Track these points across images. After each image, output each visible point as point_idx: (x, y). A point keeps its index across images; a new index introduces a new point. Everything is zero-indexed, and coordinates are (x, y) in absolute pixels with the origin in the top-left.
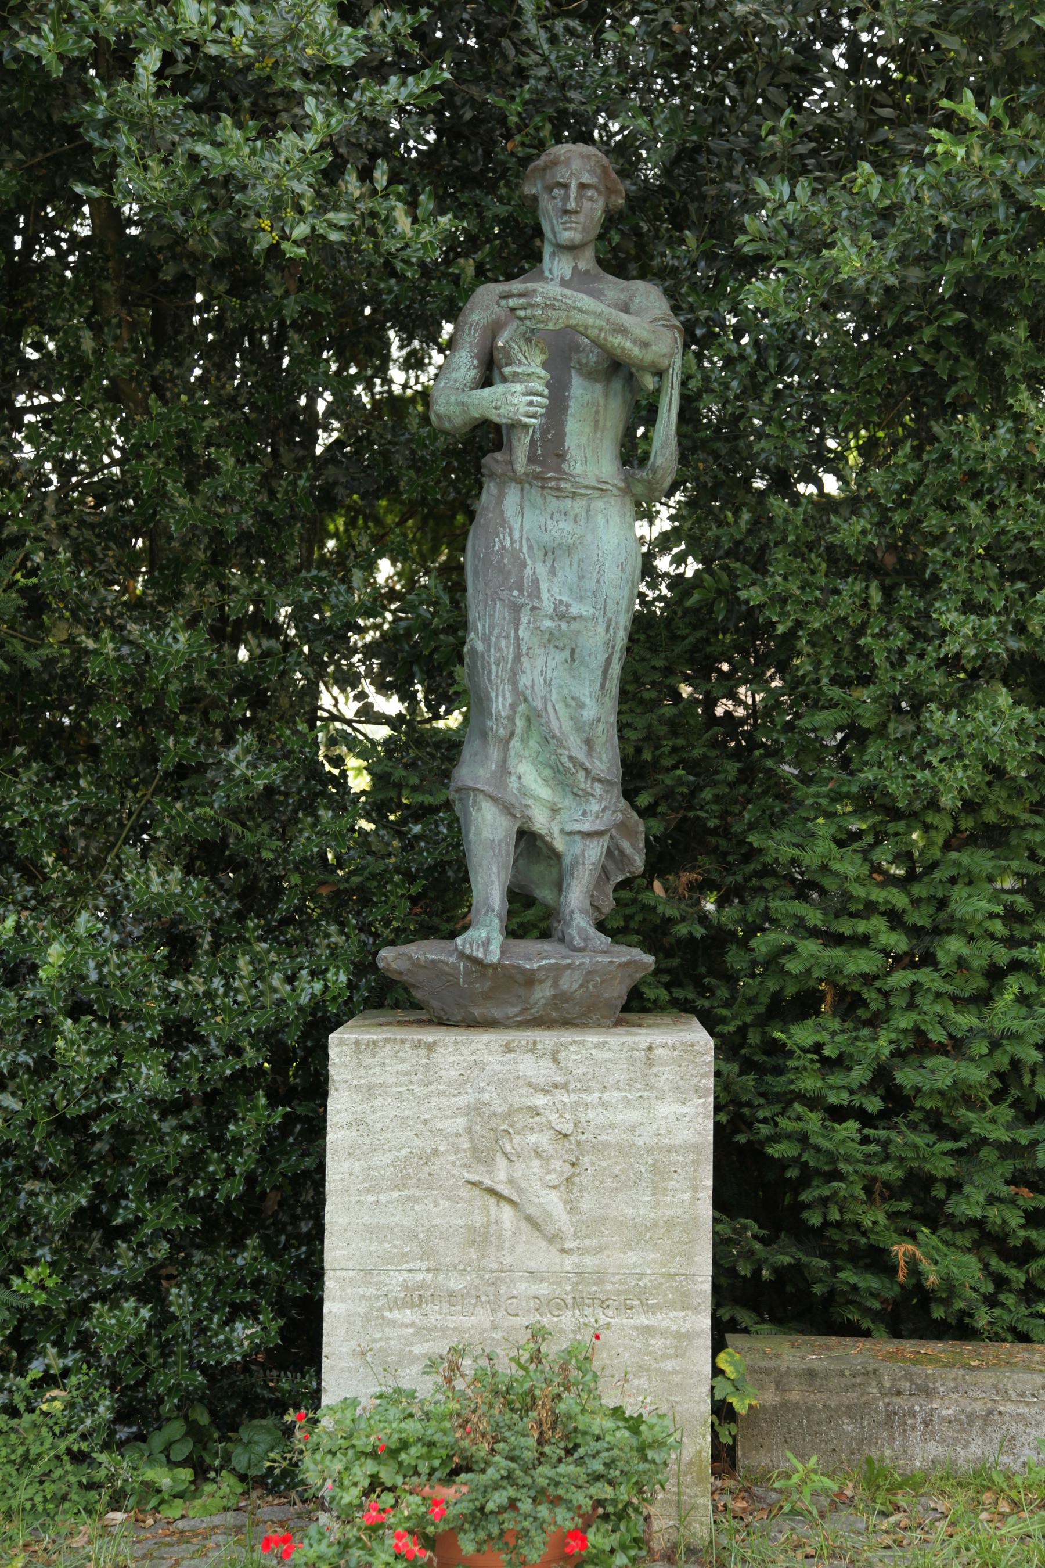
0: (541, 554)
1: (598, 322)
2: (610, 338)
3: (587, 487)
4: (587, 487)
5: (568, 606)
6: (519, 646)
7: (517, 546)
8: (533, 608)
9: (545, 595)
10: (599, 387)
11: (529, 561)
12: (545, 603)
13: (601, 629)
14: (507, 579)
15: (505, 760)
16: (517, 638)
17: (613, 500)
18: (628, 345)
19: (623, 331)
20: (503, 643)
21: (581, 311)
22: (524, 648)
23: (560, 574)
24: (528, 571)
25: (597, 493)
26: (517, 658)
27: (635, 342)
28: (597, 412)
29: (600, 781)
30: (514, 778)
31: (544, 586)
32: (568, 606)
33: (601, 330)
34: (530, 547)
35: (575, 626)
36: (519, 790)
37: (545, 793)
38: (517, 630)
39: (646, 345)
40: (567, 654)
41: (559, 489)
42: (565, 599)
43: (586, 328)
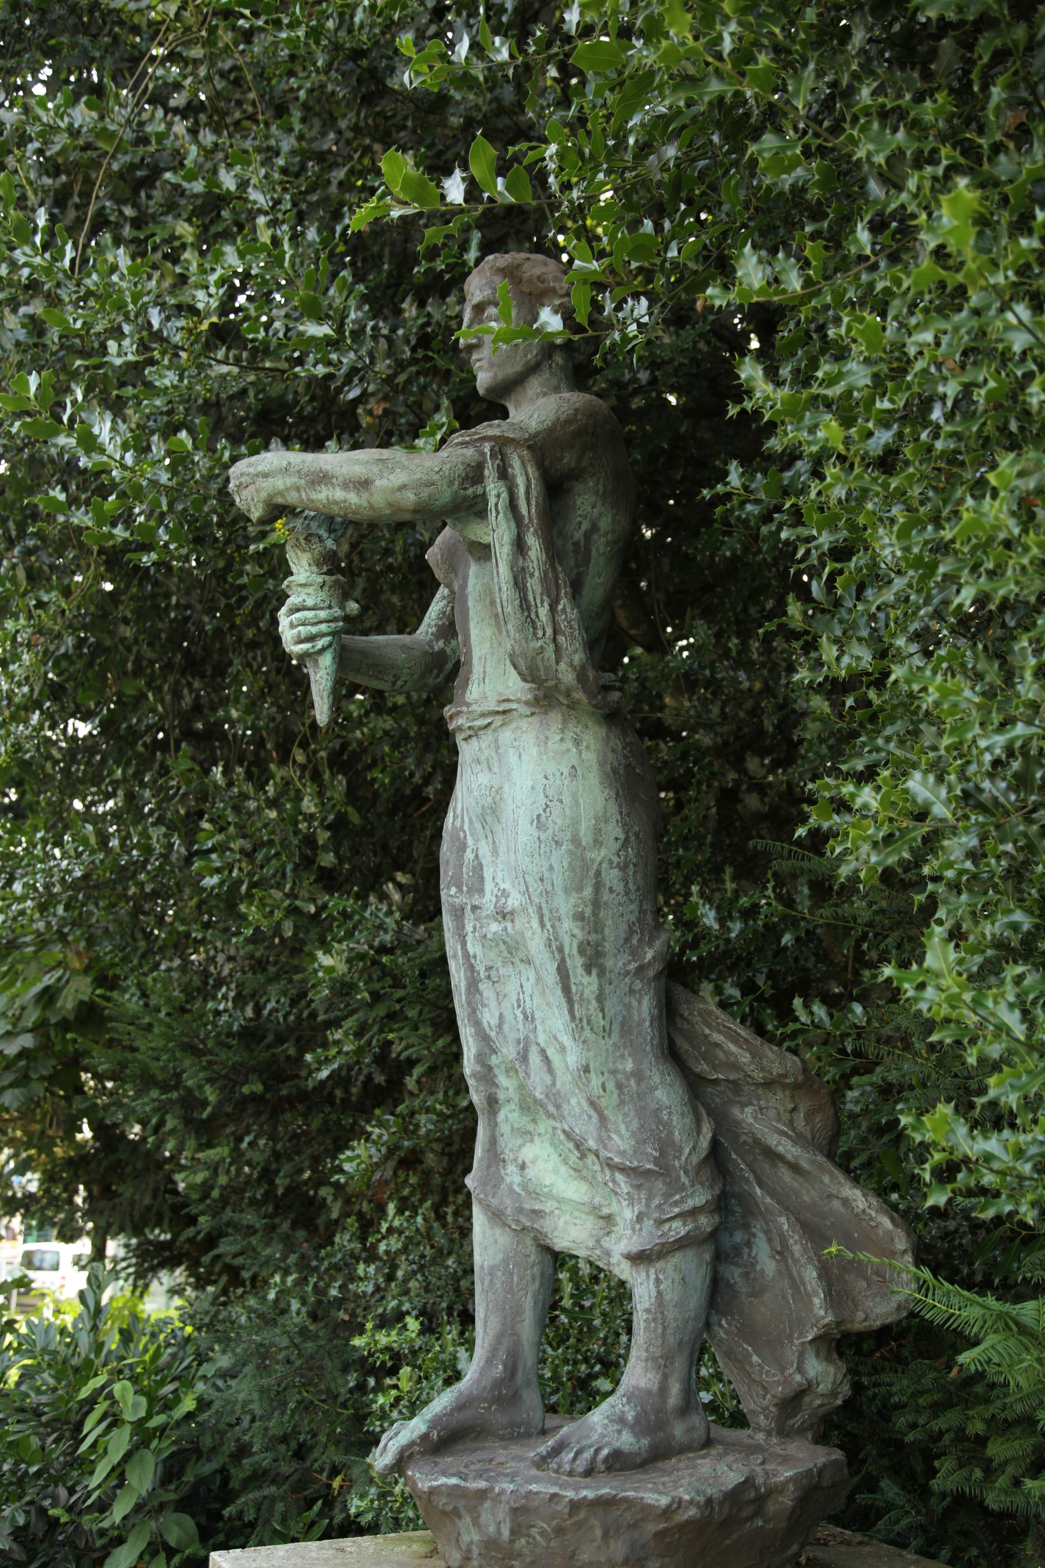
1: (290, 481)
2: (314, 496)
3: (483, 715)
4: (483, 715)
6: (471, 968)
7: (458, 824)
8: (475, 908)
9: (489, 886)
11: (470, 841)
16: (466, 955)
17: (524, 724)
18: (339, 494)
19: (323, 478)
21: (266, 475)
22: (481, 968)
24: (469, 855)
25: (498, 720)
26: (473, 985)
27: (346, 486)
30: (511, 1168)
31: (488, 873)
33: (298, 489)
34: (471, 821)
36: (524, 1186)
37: (574, 1190)
38: (464, 944)
39: (364, 484)
43: (280, 493)
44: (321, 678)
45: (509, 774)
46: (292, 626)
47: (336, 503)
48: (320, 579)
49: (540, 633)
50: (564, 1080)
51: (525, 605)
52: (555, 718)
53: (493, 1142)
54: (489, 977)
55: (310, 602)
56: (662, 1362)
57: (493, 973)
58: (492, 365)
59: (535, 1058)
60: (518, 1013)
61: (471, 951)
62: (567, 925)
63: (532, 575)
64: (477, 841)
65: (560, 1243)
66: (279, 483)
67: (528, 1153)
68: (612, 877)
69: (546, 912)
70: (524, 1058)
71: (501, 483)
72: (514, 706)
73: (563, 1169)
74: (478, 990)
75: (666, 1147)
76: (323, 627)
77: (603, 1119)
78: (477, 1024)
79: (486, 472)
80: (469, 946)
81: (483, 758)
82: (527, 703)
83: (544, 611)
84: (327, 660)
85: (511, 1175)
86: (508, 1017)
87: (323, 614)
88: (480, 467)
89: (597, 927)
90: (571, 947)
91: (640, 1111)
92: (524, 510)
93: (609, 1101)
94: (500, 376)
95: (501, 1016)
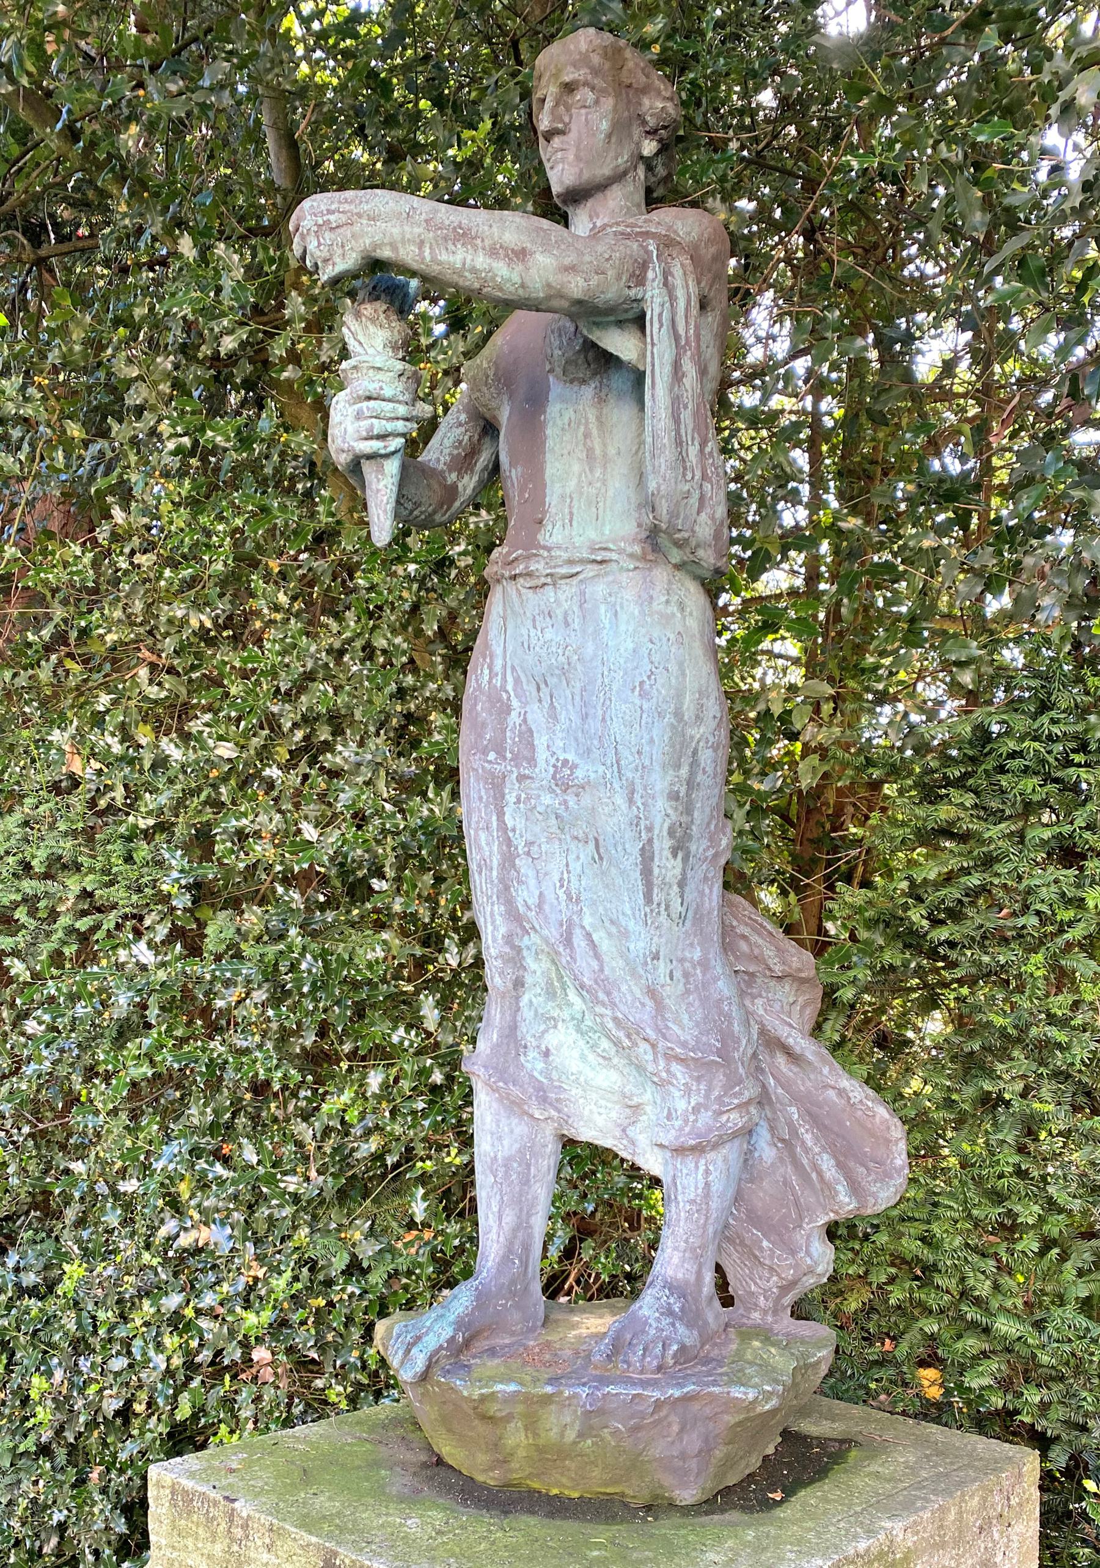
0: (533, 688)
2: (443, 257)
3: (571, 562)
4: (571, 562)
5: (574, 767)
9: (542, 755)
10: (588, 391)
11: (515, 703)
12: (541, 764)
13: (620, 800)
14: (480, 736)
15: (514, 1027)
17: (624, 578)
18: (481, 261)
20: (483, 836)
23: (562, 717)
24: (514, 718)
25: (591, 570)
26: (509, 860)
27: (492, 252)
28: (587, 435)
29: (682, 1061)
31: (541, 741)
32: (574, 767)
34: (517, 681)
35: (587, 800)
38: (501, 815)
39: (521, 255)
40: (592, 845)
41: (529, 575)
42: (571, 757)
44: (382, 488)
45: (597, 633)
46: (359, 416)
47: (474, 270)
48: (400, 366)
49: (689, 476)
50: (615, 966)
51: (679, 442)
52: (661, 575)
53: (511, 1031)
54: (528, 854)
55: (388, 392)
56: (695, 1254)
57: (534, 849)
58: (578, 158)
59: (579, 941)
60: (561, 893)
61: (510, 824)
62: (661, 804)
63: (686, 407)
64: (525, 704)
65: (585, 1134)
66: (396, 231)
67: (552, 1039)
68: (706, 757)
69: (639, 788)
70: (568, 941)
71: (664, 291)
72: (614, 556)
73: (591, 1057)
74: (514, 866)
75: (727, 1039)
76: (400, 426)
77: (660, 1006)
78: (509, 903)
79: (650, 275)
80: (508, 818)
81: (559, 613)
82: (631, 556)
83: (693, 451)
84: (392, 467)
85: (532, 1062)
86: (550, 896)
87: (402, 410)
88: (644, 266)
89: (689, 810)
90: (661, 827)
91: (704, 1000)
92: (681, 331)
93: (671, 992)
94: (586, 176)
95: (541, 894)
